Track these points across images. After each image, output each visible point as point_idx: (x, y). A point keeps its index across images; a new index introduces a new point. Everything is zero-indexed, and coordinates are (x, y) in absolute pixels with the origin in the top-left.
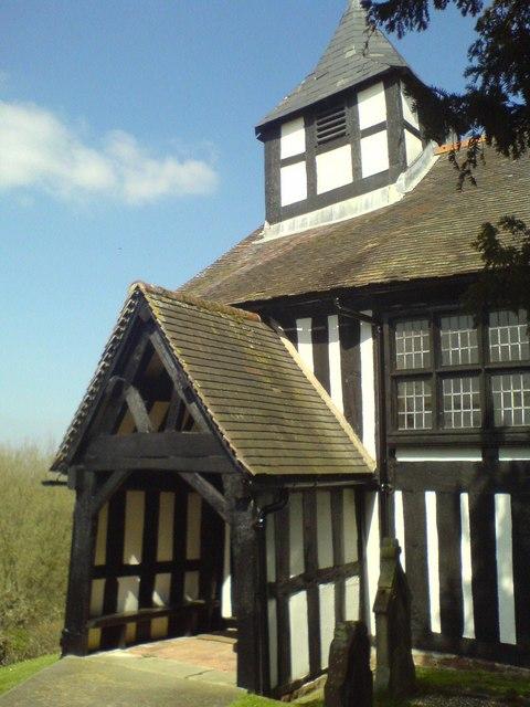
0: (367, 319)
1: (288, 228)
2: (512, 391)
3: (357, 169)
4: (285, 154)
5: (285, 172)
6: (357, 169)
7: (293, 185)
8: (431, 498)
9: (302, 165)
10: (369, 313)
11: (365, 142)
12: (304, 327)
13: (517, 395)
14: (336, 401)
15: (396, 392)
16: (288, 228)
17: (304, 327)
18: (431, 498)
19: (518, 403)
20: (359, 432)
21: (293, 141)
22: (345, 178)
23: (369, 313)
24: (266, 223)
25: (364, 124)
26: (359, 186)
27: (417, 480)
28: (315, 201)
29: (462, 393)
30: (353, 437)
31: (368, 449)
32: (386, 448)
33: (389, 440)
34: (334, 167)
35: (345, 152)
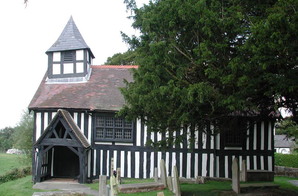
0: (90, 115)
1: (55, 82)
4: (54, 60)
5: (54, 66)
7: (56, 69)
8: (102, 151)
9: (59, 65)
11: (77, 64)
12: (76, 115)
14: (82, 130)
17: (76, 115)
18: (102, 151)
20: (87, 138)
23: (91, 114)
24: (47, 78)
25: (77, 59)
26: (75, 74)
27: (99, 148)
30: (86, 139)
31: (89, 141)
32: (93, 140)
33: (94, 140)
34: (68, 68)
35: (72, 65)
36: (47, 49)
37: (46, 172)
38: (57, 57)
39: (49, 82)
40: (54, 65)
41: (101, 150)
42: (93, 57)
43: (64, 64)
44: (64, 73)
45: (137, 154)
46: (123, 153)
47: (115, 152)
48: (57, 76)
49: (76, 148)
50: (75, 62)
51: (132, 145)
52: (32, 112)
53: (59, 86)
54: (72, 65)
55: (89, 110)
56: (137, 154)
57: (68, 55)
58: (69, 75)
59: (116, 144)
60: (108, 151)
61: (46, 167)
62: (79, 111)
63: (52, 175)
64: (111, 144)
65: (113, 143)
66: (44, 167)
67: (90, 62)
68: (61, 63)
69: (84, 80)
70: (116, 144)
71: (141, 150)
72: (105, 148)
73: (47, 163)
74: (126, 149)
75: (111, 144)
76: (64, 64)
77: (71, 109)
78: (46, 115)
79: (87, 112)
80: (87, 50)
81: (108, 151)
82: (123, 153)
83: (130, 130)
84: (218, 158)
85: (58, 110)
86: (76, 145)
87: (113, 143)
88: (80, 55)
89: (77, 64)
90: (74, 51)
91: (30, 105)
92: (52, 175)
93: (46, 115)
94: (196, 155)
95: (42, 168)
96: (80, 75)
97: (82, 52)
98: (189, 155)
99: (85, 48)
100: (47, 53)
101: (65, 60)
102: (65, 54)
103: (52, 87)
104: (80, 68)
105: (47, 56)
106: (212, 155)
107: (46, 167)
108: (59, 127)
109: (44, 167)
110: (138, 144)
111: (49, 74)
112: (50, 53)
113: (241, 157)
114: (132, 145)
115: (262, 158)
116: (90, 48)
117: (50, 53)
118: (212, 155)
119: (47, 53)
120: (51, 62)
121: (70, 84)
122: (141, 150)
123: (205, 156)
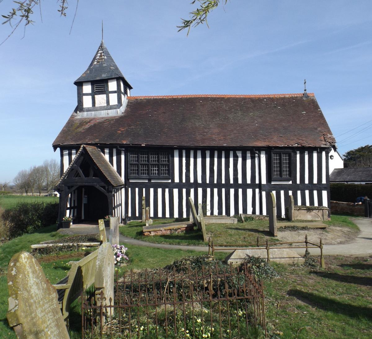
0: (123, 151)
3: (108, 102)
4: (84, 92)
5: (85, 98)
6: (108, 102)
7: (87, 102)
8: (137, 189)
9: (90, 97)
12: (107, 151)
14: (115, 168)
17: (107, 151)
18: (137, 189)
19: (156, 171)
21: (87, 89)
23: (124, 149)
31: (123, 179)
34: (101, 99)
35: (104, 96)
36: (75, 79)
37: (75, 214)
38: (87, 89)
39: (80, 116)
42: (130, 88)
43: (96, 96)
44: (97, 105)
45: (176, 191)
46: (160, 190)
47: (152, 190)
52: (58, 149)
53: (90, 120)
55: (122, 146)
56: (176, 191)
57: (100, 86)
58: (102, 108)
60: (144, 189)
61: (76, 210)
63: (83, 218)
65: (150, 180)
67: (126, 93)
68: (93, 95)
71: (180, 186)
72: (141, 186)
73: (76, 205)
74: (164, 186)
76: (96, 96)
80: (120, 79)
81: (144, 189)
82: (160, 190)
84: (264, 193)
85: (82, 146)
87: (150, 180)
88: (112, 86)
89: (110, 95)
90: (105, 81)
92: (83, 218)
94: (240, 191)
96: (112, 108)
98: (232, 191)
100: (76, 83)
101: (96, 91)
102: (97, 85)
103: (83, 122)
105: (76, 87)
106: (257, 190)
107: (76, 210)
108: (86, 165)
110: (177, 180)
111: (79, 108)
112: (79, 84)
113: (215, 183)
115: (315, 192)
117: (79, 84)
118: (257, 190)
119: (76, 83)
120: (80, 95)
122: (180, 186)
123: (249, 192)
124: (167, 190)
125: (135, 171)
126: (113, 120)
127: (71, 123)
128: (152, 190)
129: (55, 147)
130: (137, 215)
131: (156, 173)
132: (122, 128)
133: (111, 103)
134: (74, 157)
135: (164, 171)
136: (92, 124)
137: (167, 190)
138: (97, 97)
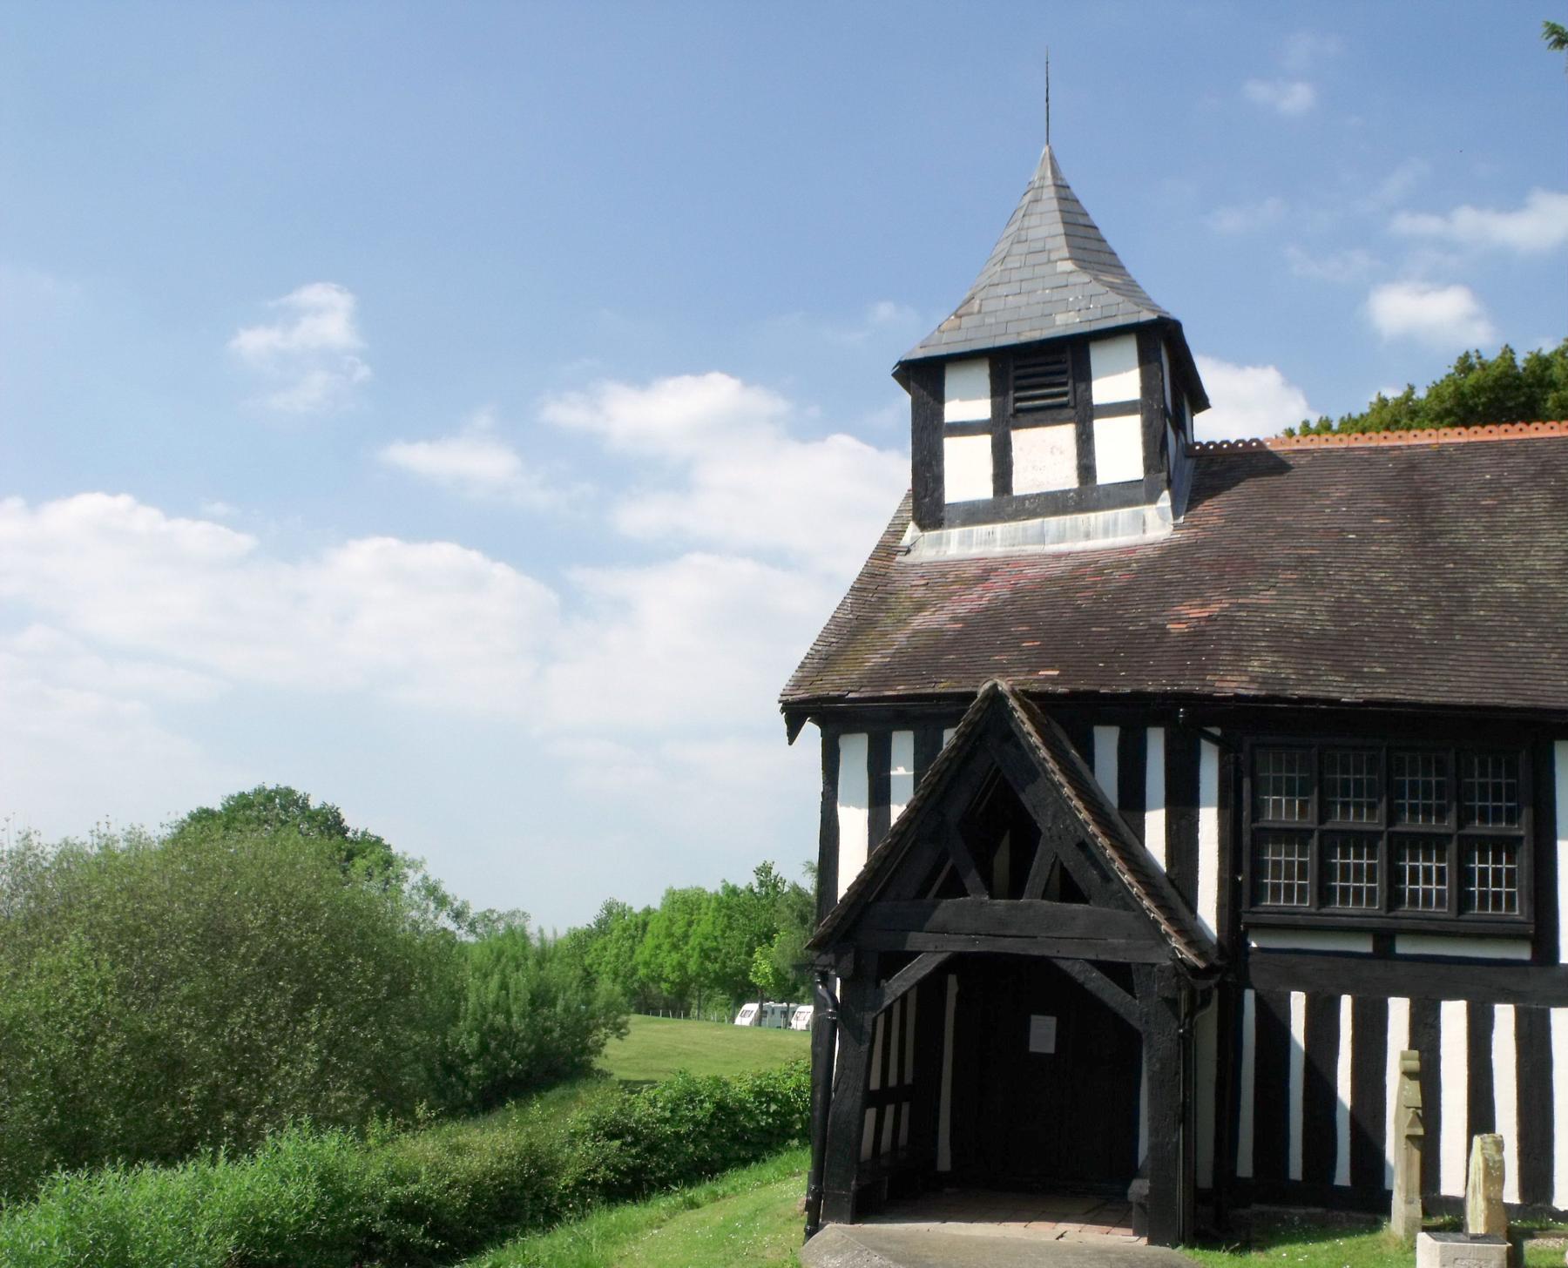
1: (955, 545)
2: (1421, 864)
3: (1086, 469)
5: (953, 447)
6: (1086, 469)
7: (966, 470)
9: (984, 442)
10: (1216, 731)
13: (1427, 871)
15: (1257, 852)
16: (955, 545)
19: (1428, 880)
21: (968, 402)
22: (1065, 477)
23: (1216, 731)
24: (912, 526)
26: (1088, 494)
28: (1004, 502)
29: (1352, 861)
33: (1246, 918)
34: (1044, 456)
35: (1065, 434)
40: (951, 445)
41: (1293, 994)
44: (1022, 484)
46: (1454, 1016)
47: (1399, 1011)
48: (974, 514)
49: (1120, 973)
50: (1084, 415)
51: (1524, 953)
52: (811, 732)
53: (986, 572)
54: (1065, 434)
57: (1039, 377)
58: (1055, 504)
59: (1403, 947)
60: (1346, 1002)
61: (906, 1108)
62: (1132, 714)
63: (944, 1163)
64: (1365, 946)
66: (890, 1109)
68: (999, 431)
69: (1155, 524)
70: (1403, 947)
73: (908, 1080)
75: (1365, 946)
77: (1073, 696)
78: (903, 747)
79: (1190, 718)
81: (1346, 1002)
82: (1454, 1016)
83: (1503, 846)
86: (1118, 948)
89: (1100, 426)
91: (797, 684)
92: (944, 1163)
93: (903, 747)
95: (871, 1114)
97: (1129, 349)
99: (1147, 316)
101: (1018, 411)
102: (1021, 372)
104: (1121, 449)
105: (903, 401)
107: (906, 1108)
109: (890, 1109)
111: (927, 505)
112: (924, 377)
114: (1524, 953)
116: (1174, 312)
121: (1058, 557)
124: (1505, 1016)
125: (1289, 876)
126: (1119, 565)
127: (877, 589)
128: (1399, 1011)
129: (795, 714)
130: (1296, 1170)
131: (1427, 893)
132: (1196, 606)
133: (1106, 474)
134: (902, 772)
135: (1484, 882)
136: (999, 588)
137: (1505, 1016)
138: (1024, 441)
